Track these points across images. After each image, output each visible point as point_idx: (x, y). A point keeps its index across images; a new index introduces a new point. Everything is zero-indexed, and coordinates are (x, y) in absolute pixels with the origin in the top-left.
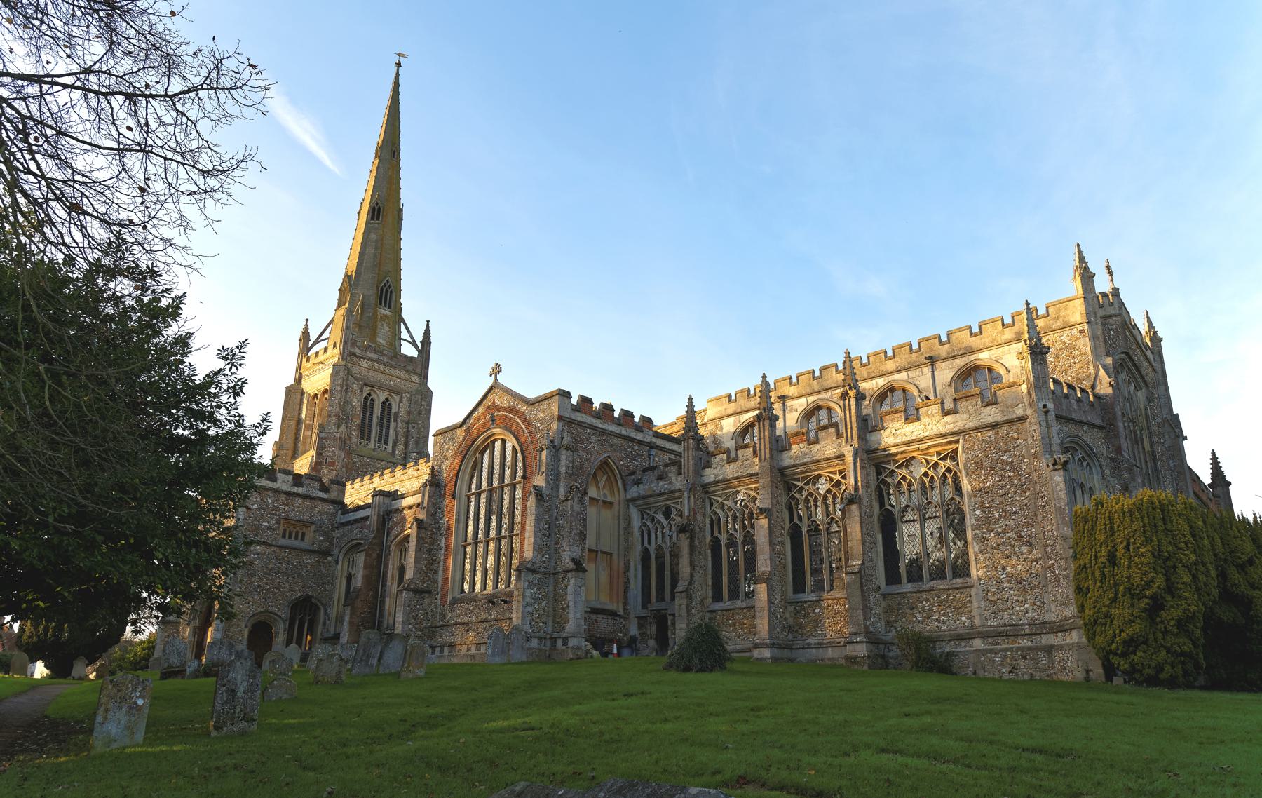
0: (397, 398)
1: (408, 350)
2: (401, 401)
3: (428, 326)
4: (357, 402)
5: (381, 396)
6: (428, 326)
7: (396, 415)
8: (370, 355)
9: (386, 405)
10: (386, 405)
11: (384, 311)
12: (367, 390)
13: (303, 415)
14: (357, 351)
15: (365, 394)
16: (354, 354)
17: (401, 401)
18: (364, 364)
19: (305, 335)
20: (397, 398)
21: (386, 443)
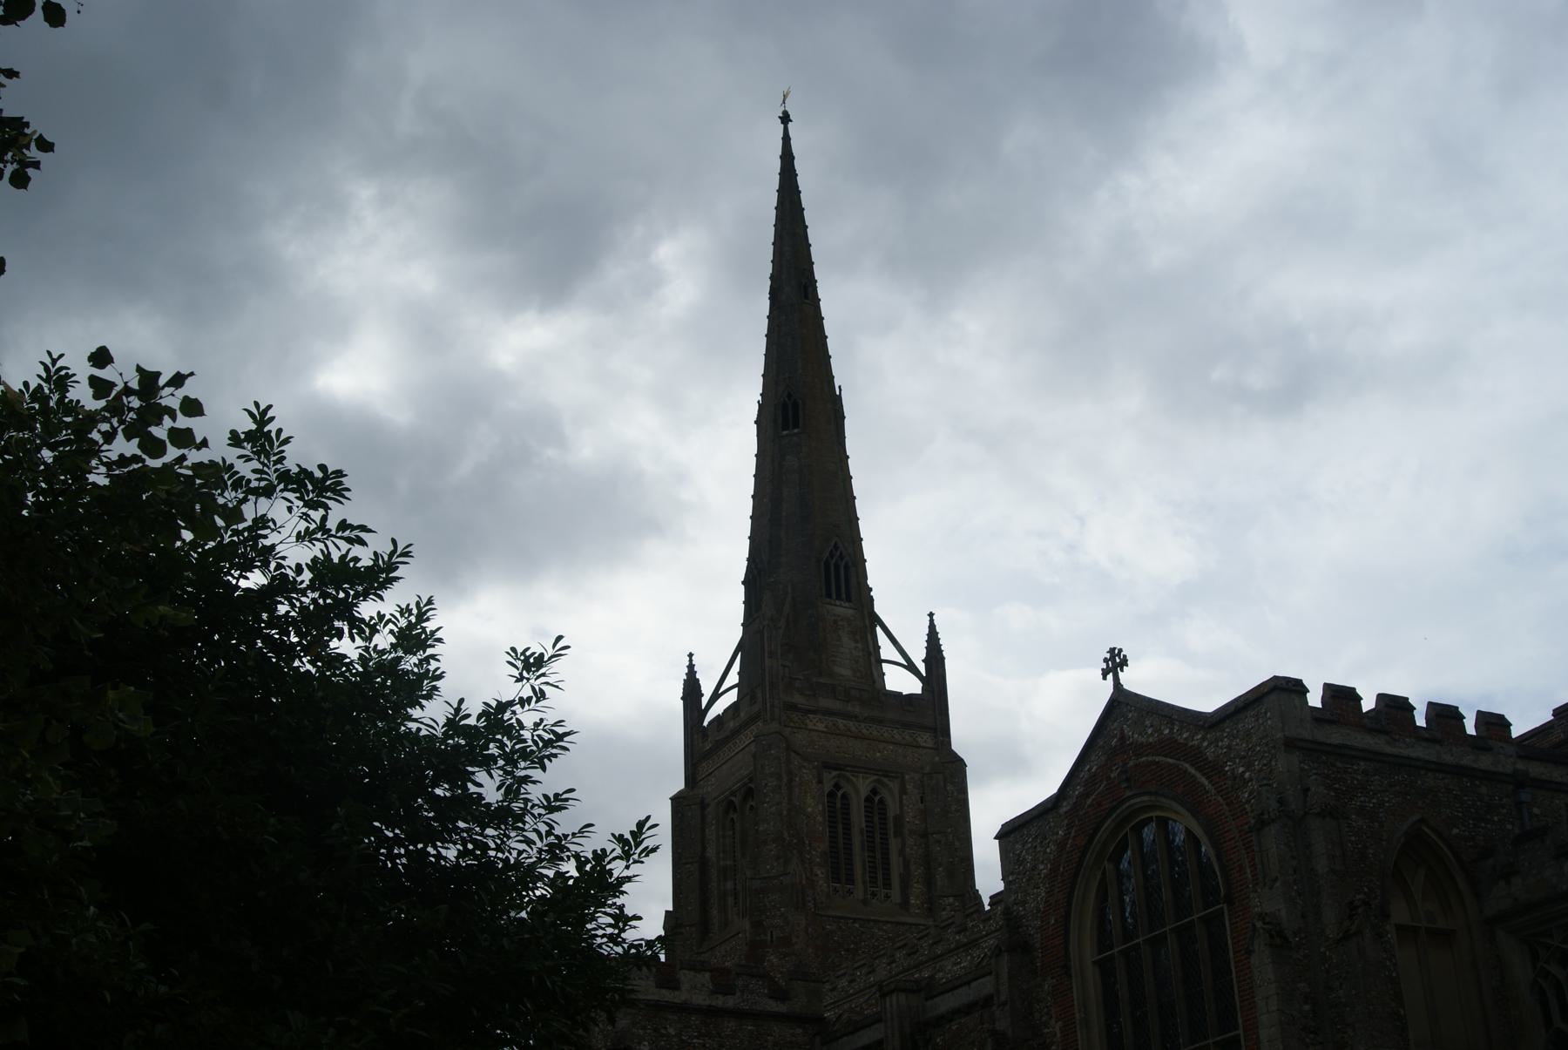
0: (894, 786)
1: (900, 682)
2: (903, 791)
3: (932, 621)
4: (813, 806)
5: (863, 785)
6: (932, 621)
7: (899, 820)
8: (825, 703)
9: (874, 804)
10: (874, 804)
11: (843, 610)
12: (830, 778)
13: (711, 852)
14: (798, 699)
15: (828, 787)
16: (793, 707)
17: (903, 791)
18: (817, 723)
19: (691, 687)
20: (894, 786)
21: (887, 884)
